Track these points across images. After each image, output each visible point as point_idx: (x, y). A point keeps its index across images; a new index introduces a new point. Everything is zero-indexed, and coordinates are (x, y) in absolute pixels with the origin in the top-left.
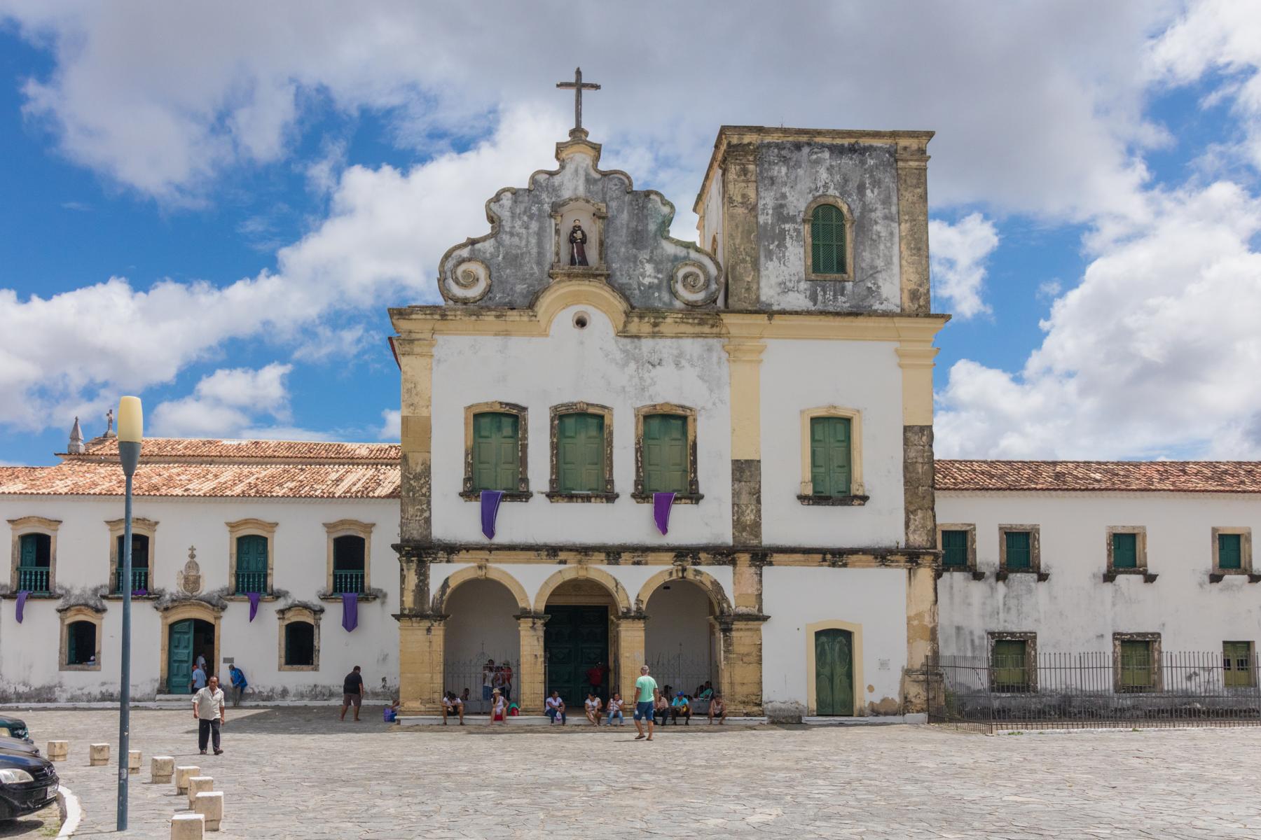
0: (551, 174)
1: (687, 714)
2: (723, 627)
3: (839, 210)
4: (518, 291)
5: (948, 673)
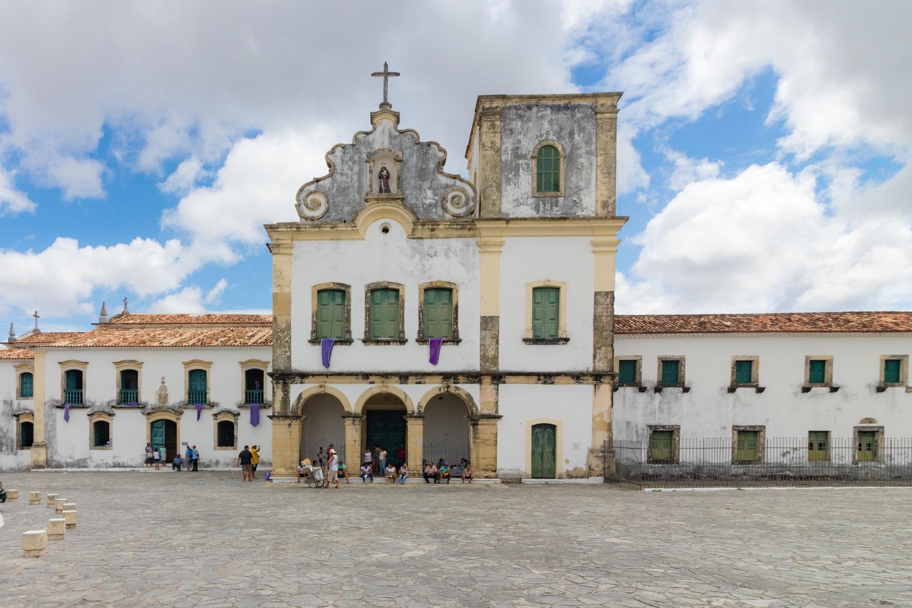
0: (367, 134)
1: (448, 477)
2: (473, 422)
3: (556, 149)
4: (346, 211)
5: (617, 450)
